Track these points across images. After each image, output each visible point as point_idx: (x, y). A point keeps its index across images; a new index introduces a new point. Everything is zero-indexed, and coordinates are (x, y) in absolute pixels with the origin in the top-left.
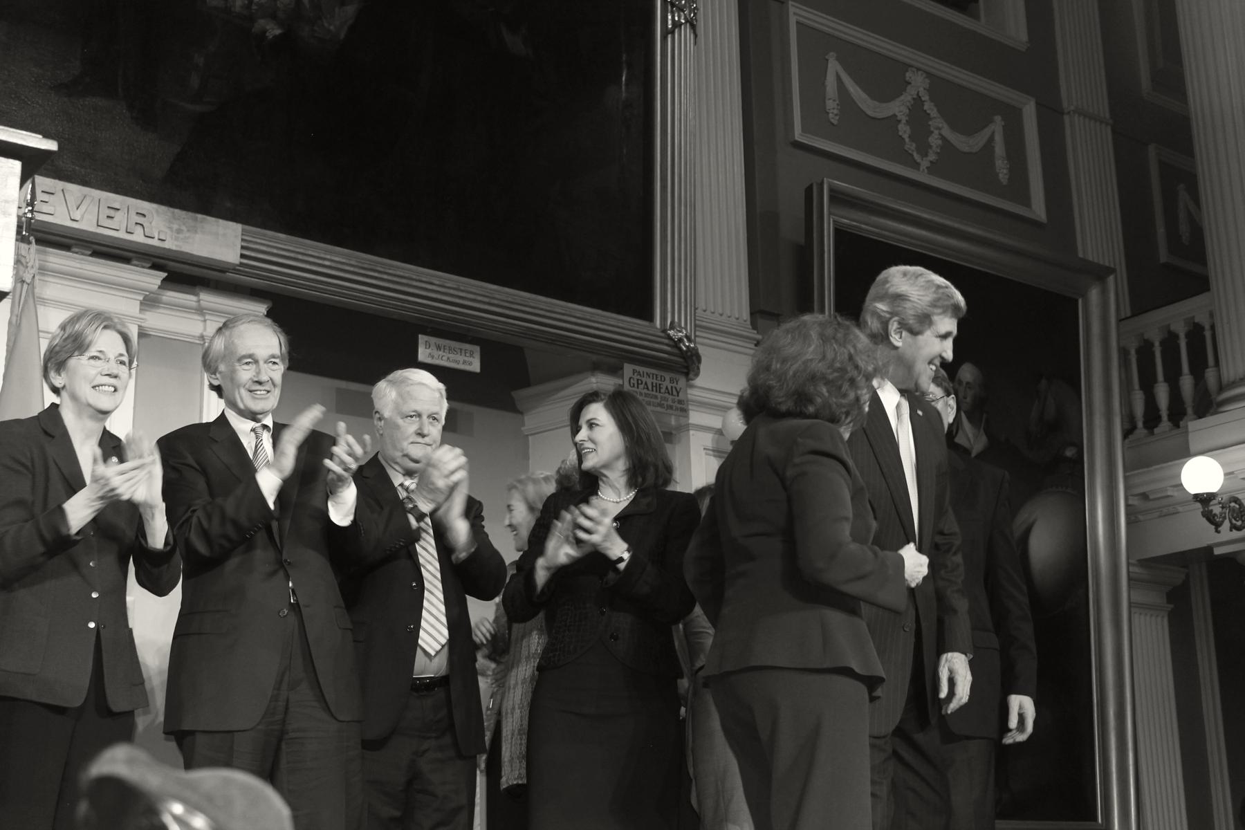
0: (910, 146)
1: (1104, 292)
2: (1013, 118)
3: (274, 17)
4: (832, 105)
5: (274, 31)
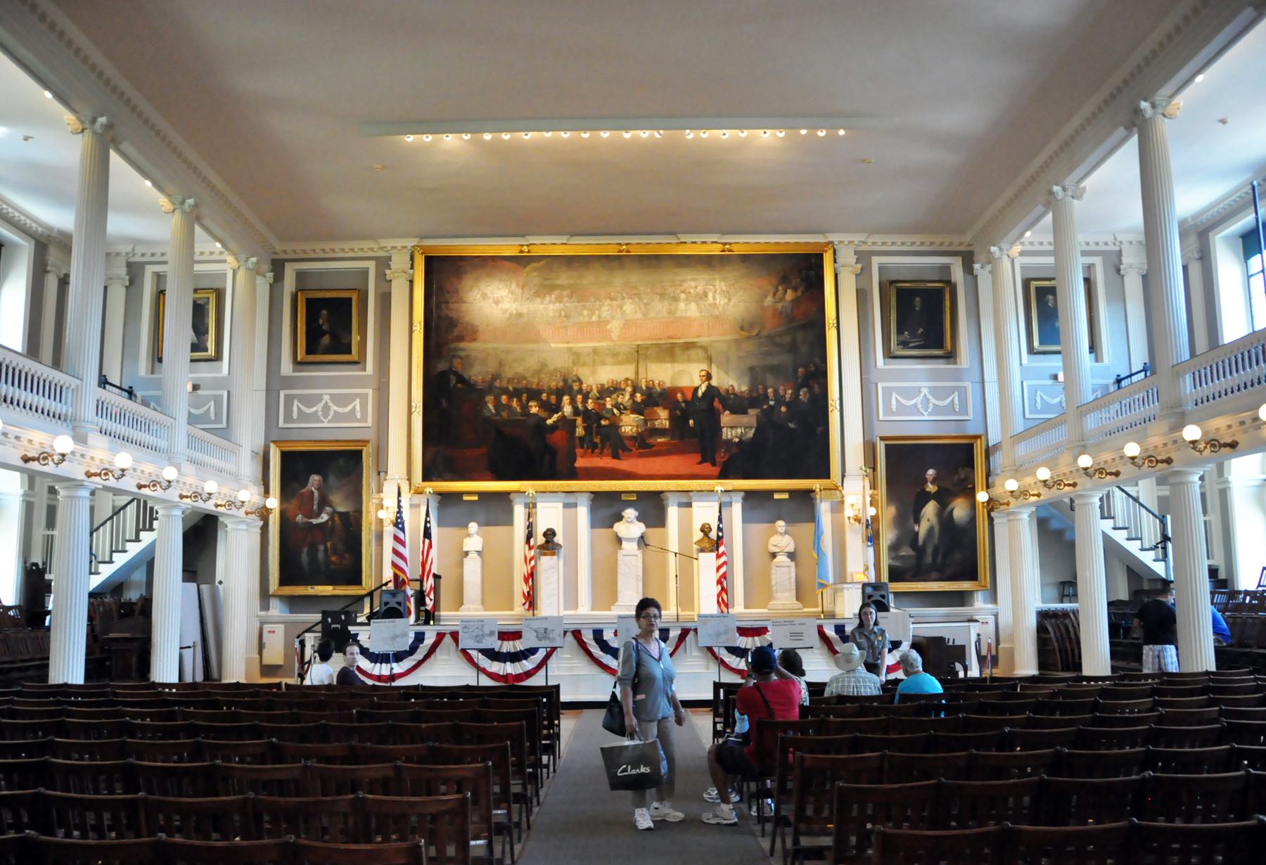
3: (737, 437)
4: (894, 407)
5: (737, 440)
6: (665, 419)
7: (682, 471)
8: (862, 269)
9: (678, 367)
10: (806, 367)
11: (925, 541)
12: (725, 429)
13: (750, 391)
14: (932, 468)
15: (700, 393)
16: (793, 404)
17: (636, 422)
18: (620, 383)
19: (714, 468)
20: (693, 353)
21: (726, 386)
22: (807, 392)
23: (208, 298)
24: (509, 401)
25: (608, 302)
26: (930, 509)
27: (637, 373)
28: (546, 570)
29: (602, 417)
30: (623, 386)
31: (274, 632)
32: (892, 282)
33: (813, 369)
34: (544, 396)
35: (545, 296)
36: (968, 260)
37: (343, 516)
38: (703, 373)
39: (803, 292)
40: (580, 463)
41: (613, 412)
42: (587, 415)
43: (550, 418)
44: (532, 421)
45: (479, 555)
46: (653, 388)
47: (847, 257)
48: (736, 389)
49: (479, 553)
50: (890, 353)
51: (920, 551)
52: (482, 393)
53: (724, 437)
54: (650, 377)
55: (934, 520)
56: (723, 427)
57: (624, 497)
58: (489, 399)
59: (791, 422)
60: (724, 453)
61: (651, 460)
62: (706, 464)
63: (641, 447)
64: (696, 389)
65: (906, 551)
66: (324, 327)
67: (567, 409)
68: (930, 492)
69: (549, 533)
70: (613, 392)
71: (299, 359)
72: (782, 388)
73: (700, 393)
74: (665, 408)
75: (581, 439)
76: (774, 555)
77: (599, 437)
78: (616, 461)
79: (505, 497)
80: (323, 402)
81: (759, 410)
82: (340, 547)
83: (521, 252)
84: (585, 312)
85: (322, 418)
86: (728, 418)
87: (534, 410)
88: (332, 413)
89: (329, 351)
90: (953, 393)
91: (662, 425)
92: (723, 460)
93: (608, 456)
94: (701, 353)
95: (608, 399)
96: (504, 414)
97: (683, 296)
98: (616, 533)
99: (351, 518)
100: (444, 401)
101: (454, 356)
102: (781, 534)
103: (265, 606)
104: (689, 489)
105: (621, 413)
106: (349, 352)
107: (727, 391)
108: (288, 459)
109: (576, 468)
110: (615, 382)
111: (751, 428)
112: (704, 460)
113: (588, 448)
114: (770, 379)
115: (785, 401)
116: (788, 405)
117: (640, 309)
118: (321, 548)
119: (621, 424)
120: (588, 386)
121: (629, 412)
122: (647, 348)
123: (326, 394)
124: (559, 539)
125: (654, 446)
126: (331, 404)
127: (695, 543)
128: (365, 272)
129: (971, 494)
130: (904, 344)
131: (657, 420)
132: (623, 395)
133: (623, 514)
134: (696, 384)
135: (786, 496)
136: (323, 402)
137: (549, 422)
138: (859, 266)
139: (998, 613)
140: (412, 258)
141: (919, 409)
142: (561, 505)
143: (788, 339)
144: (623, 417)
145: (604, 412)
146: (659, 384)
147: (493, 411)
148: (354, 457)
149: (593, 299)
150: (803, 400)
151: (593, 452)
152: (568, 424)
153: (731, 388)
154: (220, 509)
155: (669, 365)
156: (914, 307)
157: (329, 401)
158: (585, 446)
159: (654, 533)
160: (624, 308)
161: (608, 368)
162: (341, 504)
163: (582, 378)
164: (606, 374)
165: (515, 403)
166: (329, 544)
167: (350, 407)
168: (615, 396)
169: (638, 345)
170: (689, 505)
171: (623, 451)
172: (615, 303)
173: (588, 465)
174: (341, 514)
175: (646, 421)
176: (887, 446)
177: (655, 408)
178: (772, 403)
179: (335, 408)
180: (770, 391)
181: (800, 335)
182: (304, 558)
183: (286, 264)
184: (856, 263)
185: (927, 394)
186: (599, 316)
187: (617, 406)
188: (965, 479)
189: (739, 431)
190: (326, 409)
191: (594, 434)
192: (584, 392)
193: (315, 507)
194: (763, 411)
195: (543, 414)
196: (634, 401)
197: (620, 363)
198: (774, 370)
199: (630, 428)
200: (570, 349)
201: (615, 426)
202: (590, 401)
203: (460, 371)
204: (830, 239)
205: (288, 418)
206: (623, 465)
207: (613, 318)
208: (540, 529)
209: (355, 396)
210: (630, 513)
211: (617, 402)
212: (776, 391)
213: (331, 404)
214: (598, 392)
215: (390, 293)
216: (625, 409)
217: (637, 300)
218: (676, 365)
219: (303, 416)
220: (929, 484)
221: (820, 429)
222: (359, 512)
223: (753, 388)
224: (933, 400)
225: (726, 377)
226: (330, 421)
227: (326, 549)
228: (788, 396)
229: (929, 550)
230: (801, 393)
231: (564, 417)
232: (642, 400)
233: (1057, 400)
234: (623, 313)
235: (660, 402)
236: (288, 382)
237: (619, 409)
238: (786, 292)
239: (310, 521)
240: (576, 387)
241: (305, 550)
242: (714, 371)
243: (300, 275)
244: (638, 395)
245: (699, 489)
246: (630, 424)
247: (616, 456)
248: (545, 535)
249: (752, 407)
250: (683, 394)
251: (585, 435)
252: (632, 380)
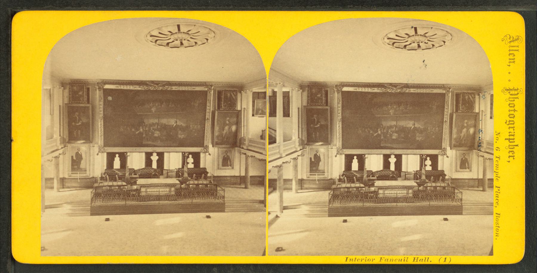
15: (174, 126)
21: (180, 124)
43: (137, 132)
48: (183, 125)
64: (174, 125)
73: (174, 126)
75: (145, 137)
95: (151, 128)
105: (154, 131)
134: (173, 123)
152: (141, 134)
164: (152, 121)
178: (191, 129)
231: (140, 132)
242: (178, 121)
247: (153, 141)
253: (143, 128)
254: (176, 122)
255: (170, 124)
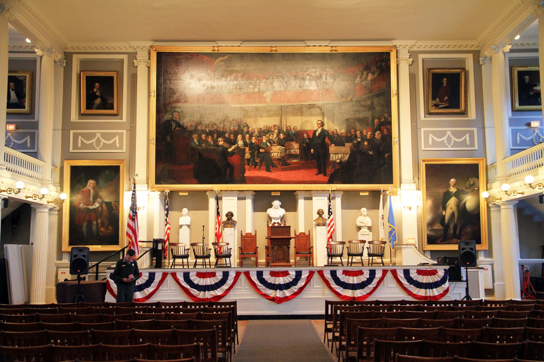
0: (447, 144)
1: (483, 162)
2: (471, 133)
3: (339, 159)
4: (430, 142)
5: (339, 161)
6: (297, 149)
7: (307, 179)
8: (413, 62)
9: (305, 118)
10: (379, 119)
11: (449, 221)
12: (332, 154)
13: (347, 133)
14: (453, 178)
15: (317, 134)
16: (371, 141)
17: (280, 150)
18: (271, 128)
19: (325, 177)
20: (313, 110)
22: (379, 134)
23: (26, 76)
24: (206, 138)
25: (264, 80)
26: (452, 202)
27: (281, 122)
28: (227, 236)
29: (260, 148)
30: (272, 130)
31: (65, 273)
32: (430, 69)
33: (383, 120)
34: (227, 135)
35: (227, 77)
36: (477, 54)
37: (108, 204)
38: (319, 122)
39: (378, 75)
40: (248, 174)
41: (267, 144)
42: (252, 147)
43: (230, 148)
44: (220, 149)
45: (188, 227)
46: (290, 131)
47: (404, 54)
48: (338, 131)
49: (189, 226)
50: (428, 111)
51: (446, 227)
52: (191, 133)
53: (331, 159)
54: (288, 125)
55: (455, 209)
56: (331, 154)
57: (273, 194)
58: (195, 136)
59: (370, 151)
60: (331, 169)
61: (289, 172)
62: (321, 175)
63: (282, 165)
64: (316, 131)
65: (438, 226)
66: (97, 94)
67: (240, 143)
68: (452, 192)
69: (229, 214)
70: (267, 133)
71: (82, 112)
72: (365, 131)
73: (317, 134)
74: (296, 143)
75: (248, 160)
76: (359, 228)
77: (259, 159)
78: (270, 173)
79: (203, 193)
80: (97, 137)
81: (352, 144)
82: (106, 222)
83: (214, 50)
84: (251, 86)
85: (96, 147)
86: (333, 148)
87: (221, 143)
88: (102, 144)
89: (99, 108)
90: (466, 134)
91: (295, 152)
92: (331, 172)
93: (264, 170)
94: (318, 110)
95: (264, 137)
96: (204, 145)
97: (308, 77)
98: (269, 215)
99: (113, 205)
100: (168, 138)
101: (175, 111)
102: (364, 215)
103: (60, 258)
104: (311, 189)
105: (272, 145)
106: (112, 108)
107: (333, 132)
108: (74, 170)
109: (245, 177)
110: (268, 127)
111: (347, 154)
112: (319, 172)
113: (252, 165)
114: (358, 125)
115: (366, 139)
116: (368, 141)
117: (283, 85)
118: (95, 223)
119: (271, 152)
120: (252, 130)
121: (275, 145)
122: (287, 107)
123: (98, 132)
124: (235, 218)
125: (290, 164)
126: (101, 139)
127: (314, 221)
128: (122, 61)
129: (477, 193)
130: (436, 106)
131: (292, 149)
132: (272, 134)
133: (273, 204)
134: (315, 129)
135: (367, 194)
136: (97, 137)
137: (230, 150)
138: (411, 60)
139: (493, 263)
140: (149, 54)
141: (445, 144)
142: (236, 198)
143: (369, 102)
144: (273, 147)
145: (262, 144)
146: (294, 128)
147: (197, 143)
148: (116, 170)
149: (255, 79)
150: (377, 138)
151: (255, 168)
153: (335, 131)
154: (29, 199)
155: (299, 117)
156: (443, 84)
157: (100, 137)
158: (251, 164)
159: (290, 215)
160: (274, 84)
161: (264, 119)
162: (106, 196)
163: (249, 125)
164: (263, 123)
165: (210, 139)
166: (99, 221)
167: (113, 140)
168: (268, 135)
169: (282, 106)
170: (311, 199)
171: (273, 167)
172: (268, 81)
173: (252, 175)
174: (107, 203)
175: (286, 150)
176: (426, 165)
177: (291, 142)
178: (359, 140)
179: (104, 141)
180: (358, 132)
181: (376, 101)
182: (84, 229)
183: (74, 55)
184: (409, 58)
185: (451, 135)
186: (259, 89)
187: (269, 141)
188: (473, 185)
189: (340, 156)
190: (98, 141)
191: (256, 158)
192: (250, 133)
193: (91, 199)
194: (354, 145)
195: (226, 145)
196: (279, 138)
197: (271, 116)
198: (360, 120)
199: (277, 153)
200: (242, 108)
201: (268, 152)
202: (254, 138)
203: (178, 120)
204: (395, 44)
205: (75, 146)
206: (273, 175)
207: (267, 90)
208: (224, 212)
209: (116, 134)
210: (277, 203)
211: (269, 139)
212: (361, 133)
213: (101, 139)
214: (258, 133)
215: (136, 75)
216: (274, 143)
217: (281, 79)
218: (303, 117)
219: (84, 146)
220: (451, 187)
221: (387, 155)
222: (118, 202)
223: (348, 131)
224: (454, 139)
225: (333, 125)
226: (99, 149)
227: (97, 223)
228: (368, 136)
229: (452, 226)
230: (376, 134)
231: (238, 147)
232: (283, 137)
233: (530, 138)
234: (274, 87)
235: (294, 139)
236: (75, 126)
237: (270, 143)
238: (368, 75)
239: (88, 207)
240: (245, 130)
241: (85, 224)
242: (326, 121)
243: (83, 63)
244: (282, 135)
245: (317, 189)
246: (276, 151)
247: (268, 170)
248: (227, 215)
249: (348, 142)
250: (308, 135)
251: (251, 158)
252: (278, 126)
253: (243, 138)
254: (322, 124)
255: (308, 127)
